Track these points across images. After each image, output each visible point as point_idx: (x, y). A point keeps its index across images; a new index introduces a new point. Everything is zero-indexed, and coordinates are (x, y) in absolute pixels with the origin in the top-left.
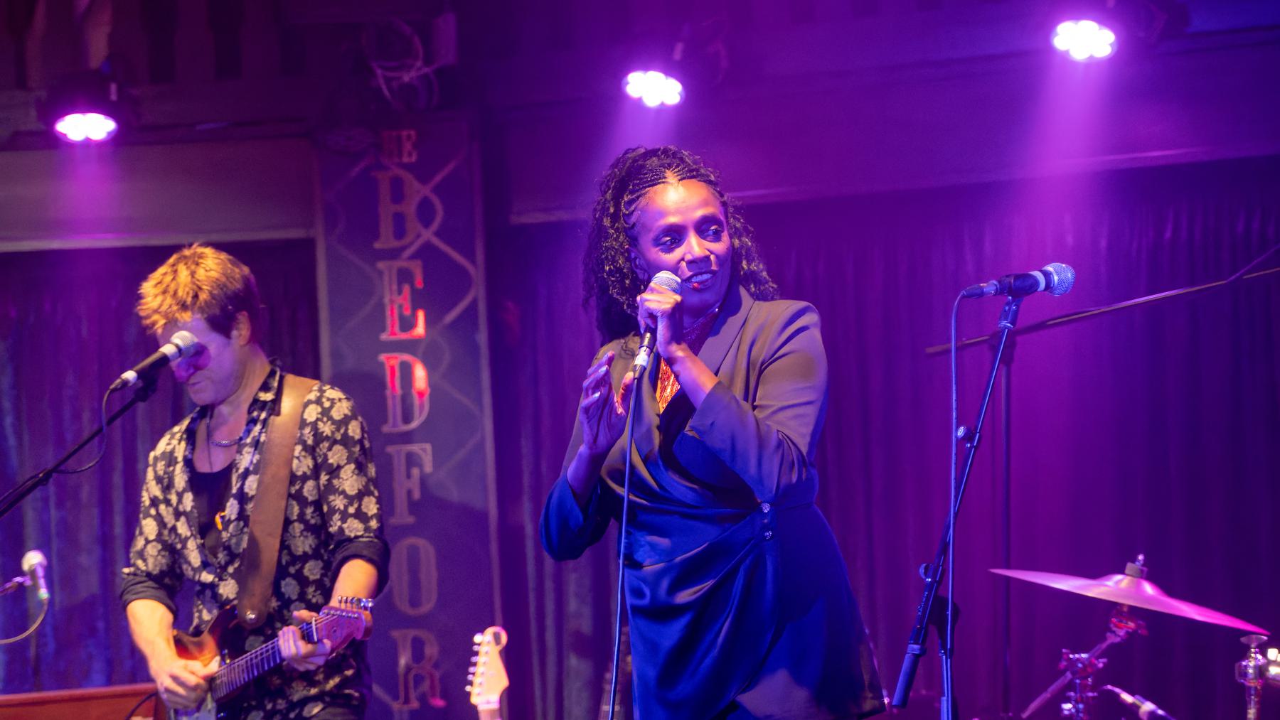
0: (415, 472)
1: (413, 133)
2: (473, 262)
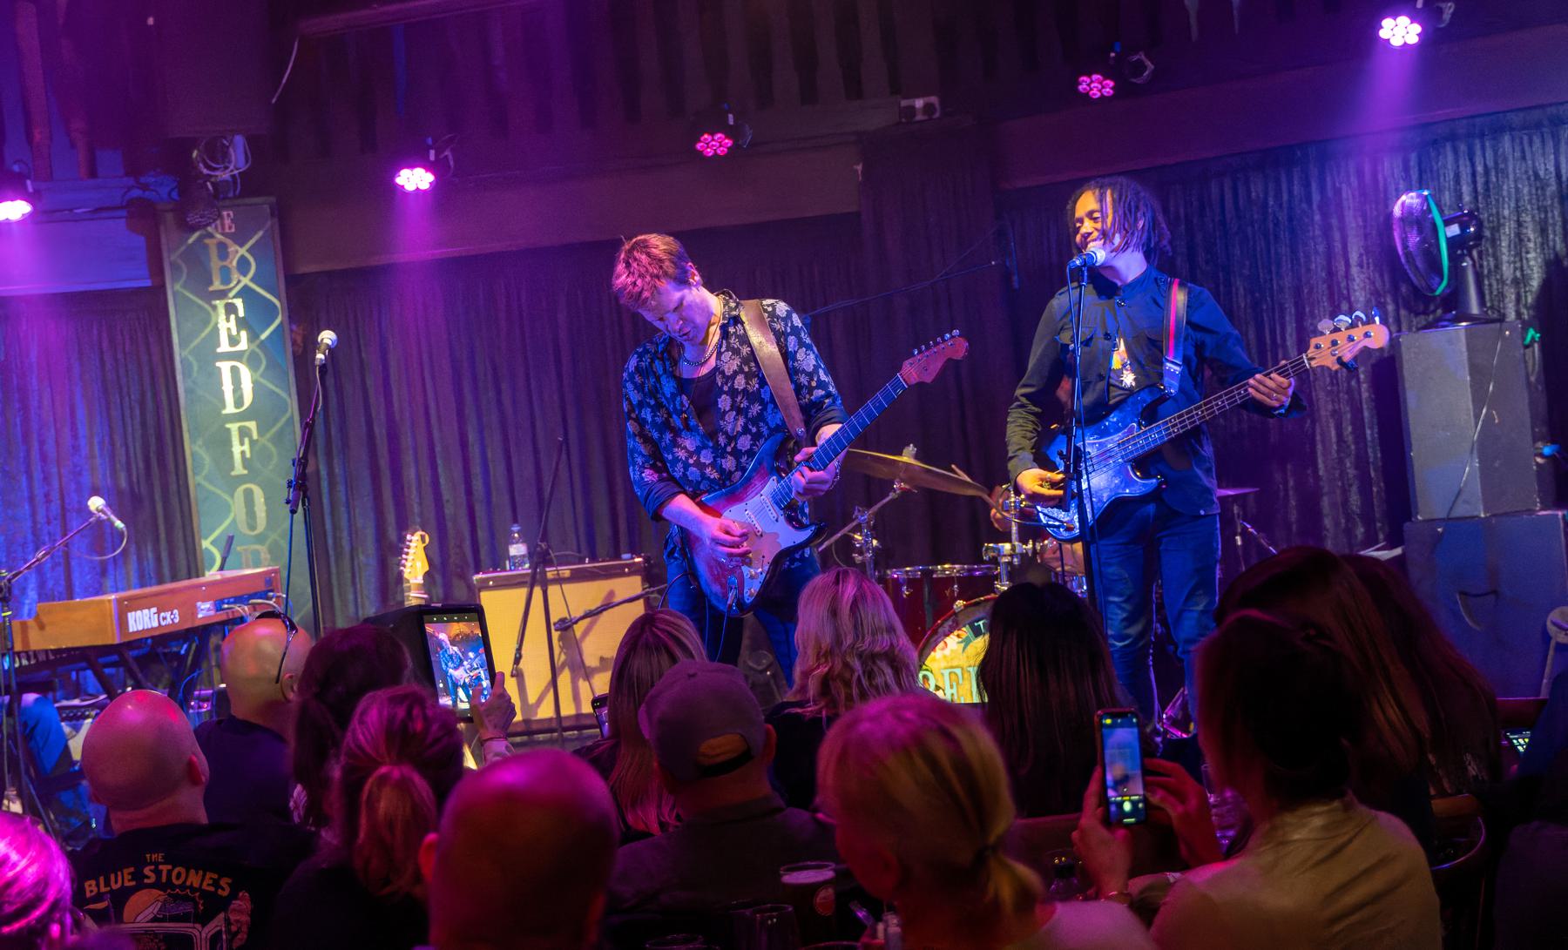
0: (246, 440)
1: (231, 213)
2: (280, 301)
